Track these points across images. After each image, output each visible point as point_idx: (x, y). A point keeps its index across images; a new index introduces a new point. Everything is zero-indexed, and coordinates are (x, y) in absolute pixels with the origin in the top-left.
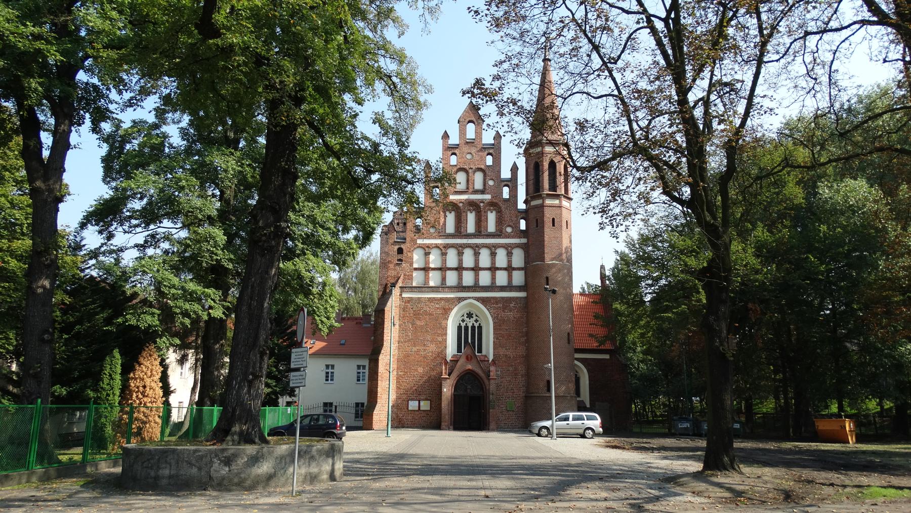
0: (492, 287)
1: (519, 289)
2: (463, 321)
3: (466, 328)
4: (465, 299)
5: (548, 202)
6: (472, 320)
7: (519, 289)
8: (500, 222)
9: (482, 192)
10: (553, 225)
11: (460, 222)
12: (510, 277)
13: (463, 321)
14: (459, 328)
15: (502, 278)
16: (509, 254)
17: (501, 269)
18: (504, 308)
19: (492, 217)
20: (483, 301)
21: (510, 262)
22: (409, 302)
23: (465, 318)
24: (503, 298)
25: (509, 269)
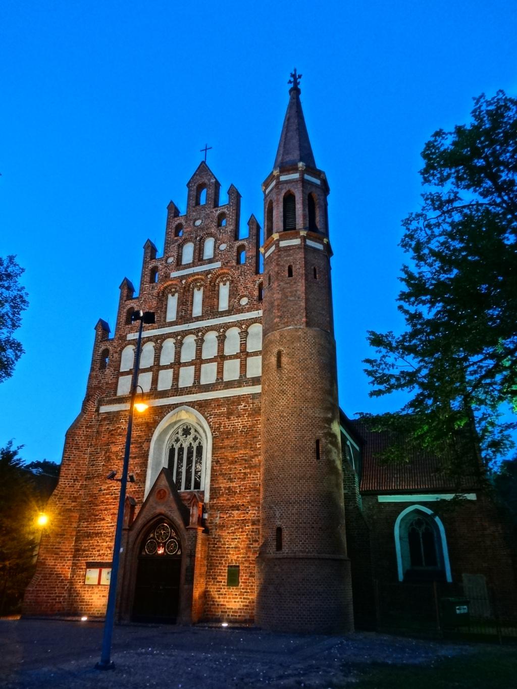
0: (221, 384)
1: (255, 381)
2: (177, 440)
3: (181, 449)
4: (176, 406)
5: (283, 244)
6: (190, 438)
7: (255, 381)
8: (233, 294)
9: (210, 261)
10: (290, 274)
11: (185, 303)
12: (243, 367)
13: (177, 440)
14: (172, 451)
15: (232, 371)
16: (244, 335)
17: (231, 357)
18: (229, 414)
19: (224, 291)
20: (201, 406)
21: (243, 345)
22: (104, 419)
23: (179, 436)
24: (227, 399)
25: (244, 354)
